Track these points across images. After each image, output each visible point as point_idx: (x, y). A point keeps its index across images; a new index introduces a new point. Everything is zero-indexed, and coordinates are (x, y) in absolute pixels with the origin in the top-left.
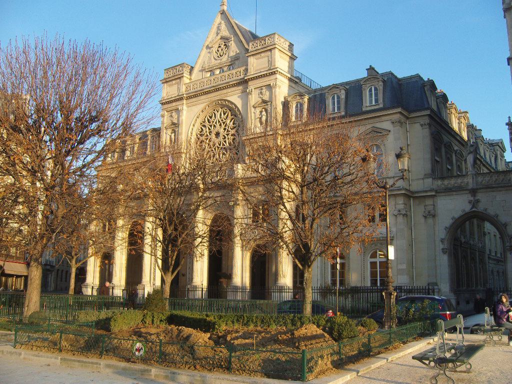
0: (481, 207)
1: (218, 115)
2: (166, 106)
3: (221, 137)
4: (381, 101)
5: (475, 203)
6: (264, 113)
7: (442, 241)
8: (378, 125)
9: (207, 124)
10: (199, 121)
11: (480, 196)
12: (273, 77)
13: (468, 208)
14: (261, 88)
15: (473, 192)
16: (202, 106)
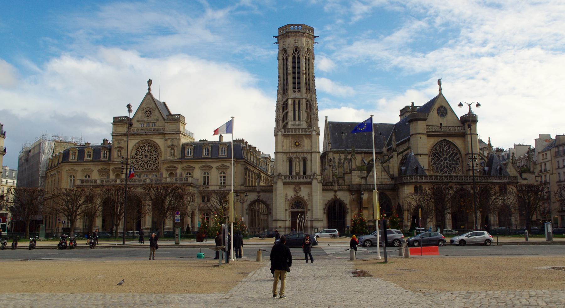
0: (260, 198)
1: (147, 146)
2: (115, 137)
3: (148, 158)
4: (226, 154)
5: (259, 197)
6: (173, 151)
7: (246, 210)
8: (225, 164)
9: (140, 150)
10: (135, 148)
11: (261, 194)
12: (178, 135)
13: (256, 198)
14: (172, 139)
15: (259, 192)
16: (137, 141)
